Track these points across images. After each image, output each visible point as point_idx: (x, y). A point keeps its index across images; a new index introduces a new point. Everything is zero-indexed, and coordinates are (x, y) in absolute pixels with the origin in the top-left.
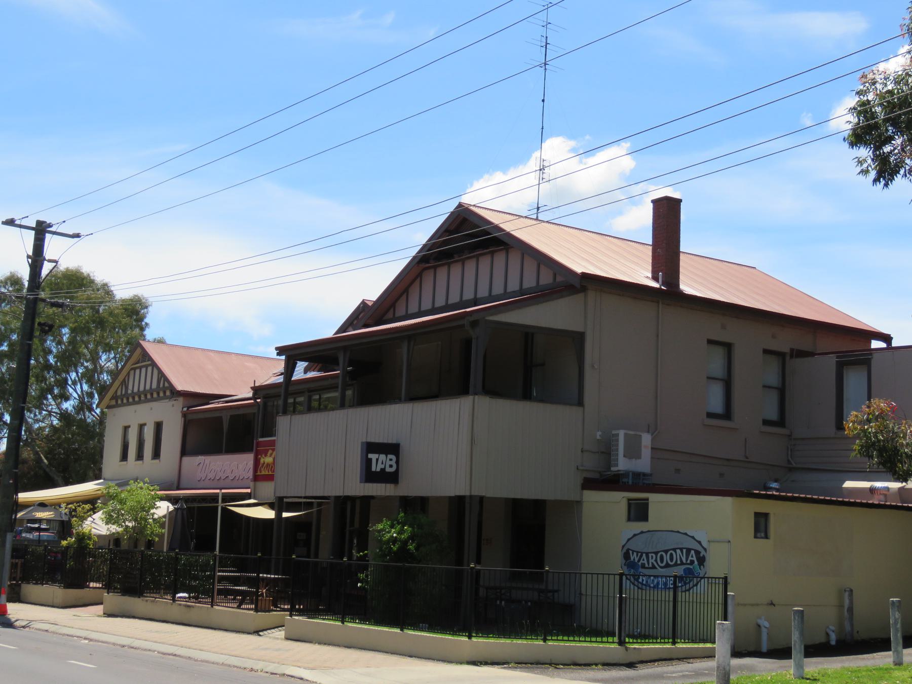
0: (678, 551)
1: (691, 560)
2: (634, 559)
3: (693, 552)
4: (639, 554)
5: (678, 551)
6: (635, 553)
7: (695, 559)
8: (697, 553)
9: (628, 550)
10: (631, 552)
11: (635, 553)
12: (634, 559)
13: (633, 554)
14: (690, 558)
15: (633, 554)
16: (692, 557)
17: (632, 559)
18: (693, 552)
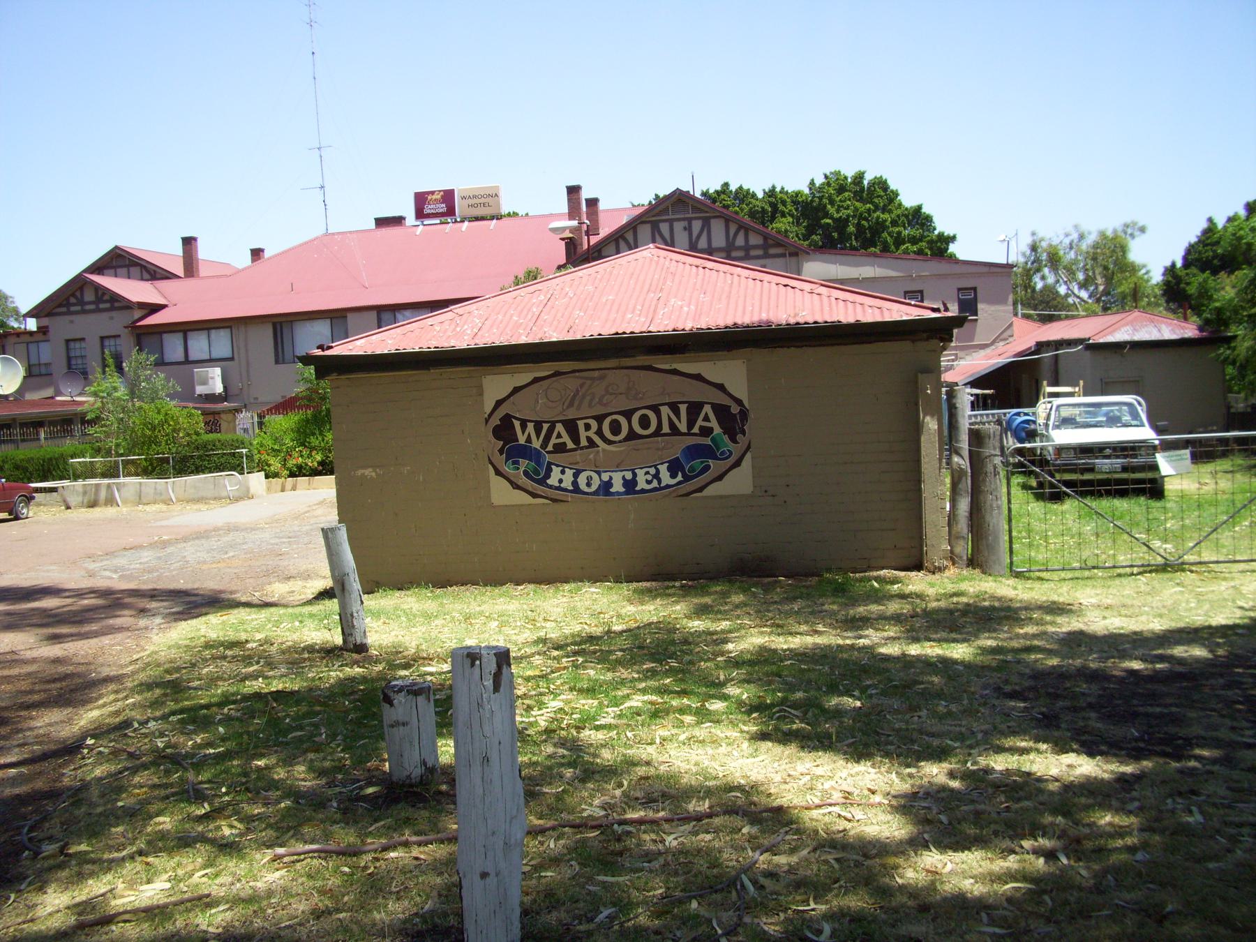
0: (665, 411)
1: (701, 428)
2: (529, 440)
3: (707, 409)
4: (546, 426)
5: (665, 411)
6: (530, 426)
7: (714, 423)
8: (721, 411)
9: (507, 420)
10: (517, 424)
11: (530, 426)
12: (529, 440)
13: (524, 427)
14: (700, 422)
15: (524, 427)
16: (706, 419)
17: (522, 440)
18: (707, 409)
